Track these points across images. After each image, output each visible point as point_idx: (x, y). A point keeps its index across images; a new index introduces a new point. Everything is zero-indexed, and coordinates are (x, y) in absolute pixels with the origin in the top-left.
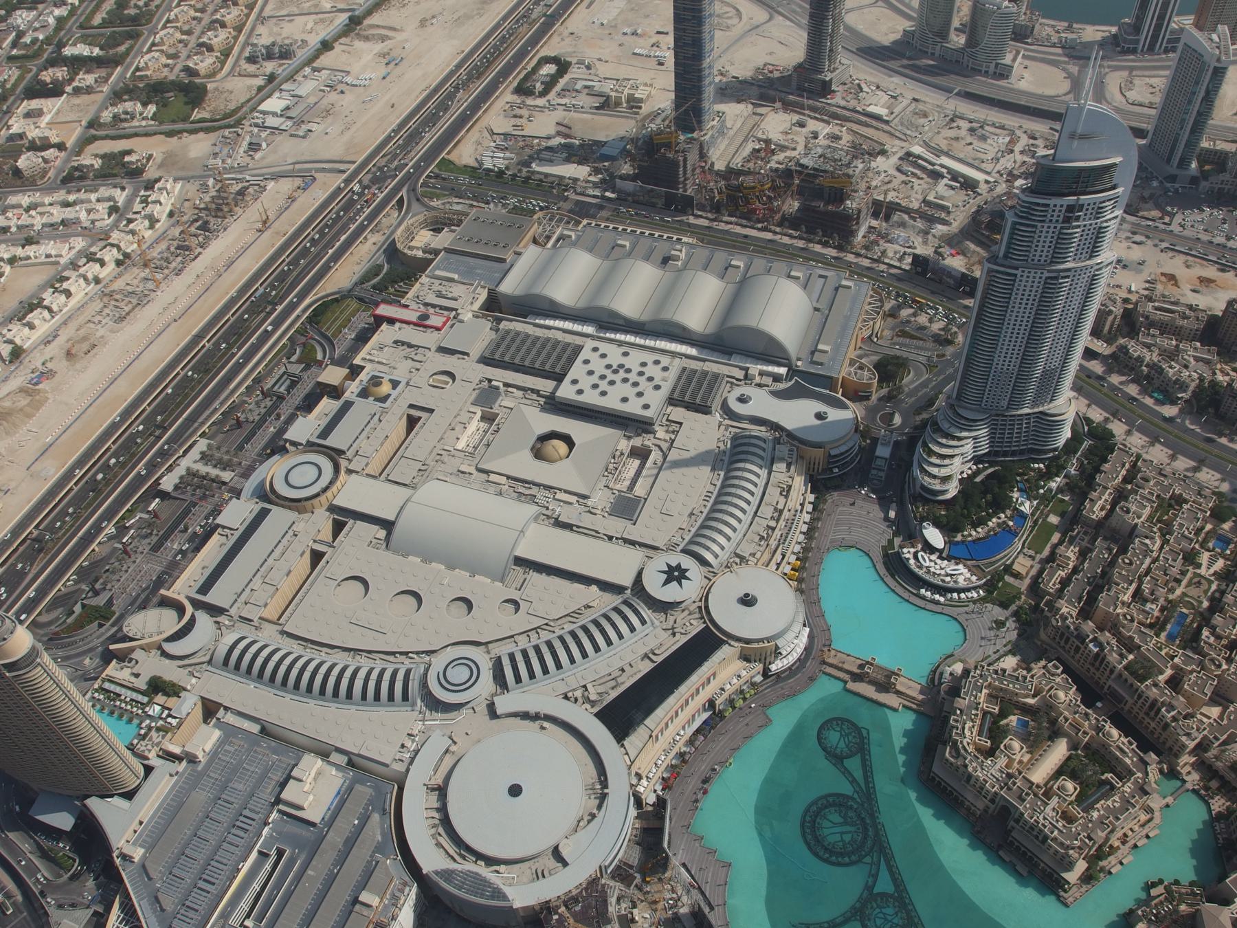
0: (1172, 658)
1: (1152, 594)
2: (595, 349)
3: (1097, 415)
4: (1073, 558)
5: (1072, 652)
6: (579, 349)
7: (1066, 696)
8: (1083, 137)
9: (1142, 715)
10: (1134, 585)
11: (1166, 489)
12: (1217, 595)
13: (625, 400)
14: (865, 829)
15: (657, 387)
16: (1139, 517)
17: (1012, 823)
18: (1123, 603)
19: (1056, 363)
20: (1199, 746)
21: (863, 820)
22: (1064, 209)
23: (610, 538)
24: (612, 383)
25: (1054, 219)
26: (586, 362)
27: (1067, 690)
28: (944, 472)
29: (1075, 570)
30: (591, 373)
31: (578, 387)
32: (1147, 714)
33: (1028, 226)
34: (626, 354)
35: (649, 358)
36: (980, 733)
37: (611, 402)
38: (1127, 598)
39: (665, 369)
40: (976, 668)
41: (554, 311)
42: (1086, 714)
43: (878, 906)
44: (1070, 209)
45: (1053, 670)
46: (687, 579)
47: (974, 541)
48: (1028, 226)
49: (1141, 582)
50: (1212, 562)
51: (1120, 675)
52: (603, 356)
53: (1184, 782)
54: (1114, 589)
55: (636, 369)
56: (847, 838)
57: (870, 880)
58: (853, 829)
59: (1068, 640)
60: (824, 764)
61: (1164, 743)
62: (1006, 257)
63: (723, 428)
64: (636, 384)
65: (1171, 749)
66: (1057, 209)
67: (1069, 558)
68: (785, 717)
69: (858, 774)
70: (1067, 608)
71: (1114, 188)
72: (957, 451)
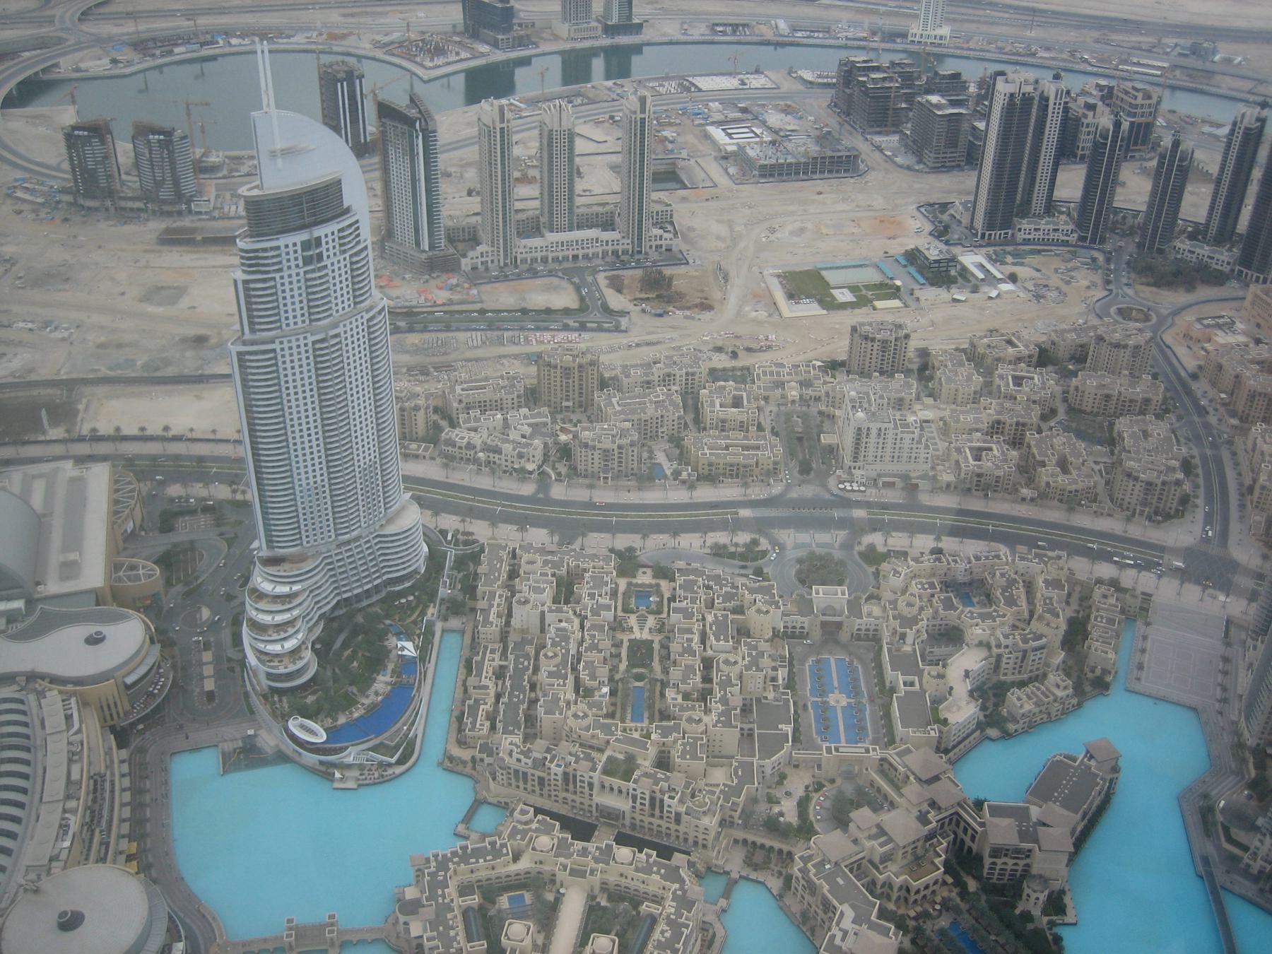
0: (648, 736)
1: (593, 677)
3: (449, 522)
4: (491, 684)
5: (537, 789)
8: (287, 152)
9: (647, 819)
10: (571, 678)
11: (557, 565)
12: (664, 652)
20: (722, 823)
22: (299, 248)
25: (293, 264)
27: (548, 831)
28: (290, 644)
29: (498, 697)
32: (653, 815)
33: (264, 281)
36: (470, 939)
38: (571, 696)
40: (428, 860)
42: (585, 849)
44: (306, 245)
48: (264, 281)
49: (574, 669)
50: (642, 621)
53: (728, 873)
61: (686, 840)
62: (253, 331)
65: (696, 843)
66: (291, 249)
67: (486, 687)
71: (348, 210)
72: (296, 613)
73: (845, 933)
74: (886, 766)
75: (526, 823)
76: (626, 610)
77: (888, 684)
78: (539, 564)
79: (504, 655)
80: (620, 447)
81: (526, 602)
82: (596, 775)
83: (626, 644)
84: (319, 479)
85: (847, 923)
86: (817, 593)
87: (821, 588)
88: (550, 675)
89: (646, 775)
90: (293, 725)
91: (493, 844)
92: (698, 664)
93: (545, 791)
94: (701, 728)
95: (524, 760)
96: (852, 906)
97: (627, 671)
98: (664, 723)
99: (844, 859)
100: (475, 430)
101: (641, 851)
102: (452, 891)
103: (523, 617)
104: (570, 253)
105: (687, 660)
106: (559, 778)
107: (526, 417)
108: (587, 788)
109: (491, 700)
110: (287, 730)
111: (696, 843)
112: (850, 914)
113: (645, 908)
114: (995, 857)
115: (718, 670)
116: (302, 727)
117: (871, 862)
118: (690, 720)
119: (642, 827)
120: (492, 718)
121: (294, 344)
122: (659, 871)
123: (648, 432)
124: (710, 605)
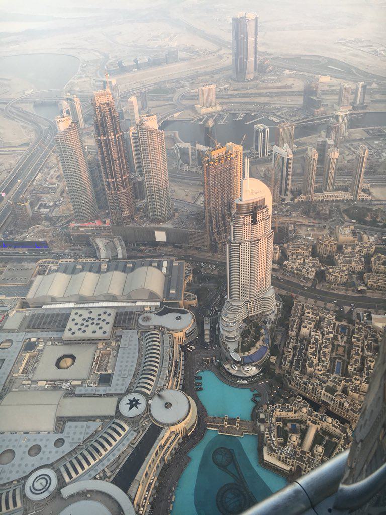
0: (341, 381)
2: (77, 314)
3: (284, 292)
4: (291, 351)
5: (303, 390)
6: (68, 315)
9: (337, 408)
13: (94, 332)
15: (108, 323)
17: (303, 472)
19: (264, 276)
23: (100, 395)
24: (87, 326)
26: (74, 320)
27: (306, 406)
29: (294, 356)
30: (76, 324)
31: (72, 332)
32: (339, 407)
34: (91, 312)
35: (101, 311)
37: (89, 334)
39: (109, 315)
41: (54, 300)
45: (299, 400)
46: (139, 404)
49: (319, 352)
51: (324, 394)
52: (81, 316)
55: (96, 318)
59: (300, 385)
63: (139, 334)
64: (98, 324)
67: (290, 352)
68: (197, 454)
71: (266, 207)
75: (299, 402)
76: (337, 333)
79: (297, 342)
80: (341, 275)
81: (306, 327)
82: (323, 392)
84: (247, 282)
88: (311, 354)
89: (339, 395)
92: (359, 358)
94: (359, 382)
95: (300, 380)
100: (294, 262)
101: (335, 420)
102: (274, 420)
103: (304, 331)
104: (331, 199)
105: (356, 357)
107: (311, 260)
109: (291, 356)
111: (353, 420)
113: (334, 439)
115: (367, 363)
118: (356, 379)
120: (291, 362)
121: (245, 245)
123: (351, 272)
124: (366, 337)
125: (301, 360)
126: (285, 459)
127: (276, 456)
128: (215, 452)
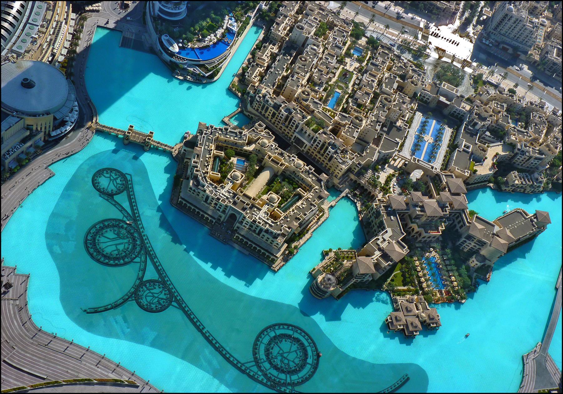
5: (270, 117)
7: (269, 142)
9: (315, 153)
10: (308, 75)
14: (134, 240)
16: (309, 34)
18: (302, 85)
21: (132, 234)
29: (269, 67)
32: (319, 152)
38: (304, 82)
43: (148, 289)
47: (200, 49)
51: (302, 130)
54: (296, 76)
56: (121, 247)
57: (141, 273)
58: (126, 241)
59: (267, 108)
60: (99, 200)
65: (332, 173)
69: (126, 205)
70: (266, 90)
73: (384, 240)
74: (437, 177)
77: (456, 143)
78: (316, 12)
83: (340, 70)
85: (387, 237)
86: (444, 86)
87: (447, 85)
90: (164, 38)
91: (241, 133)
93: (273, 120)
96: (393, 231)
97: (336, 82)
98: (344, 114)
99: (398, 210)
106: (283, 117)
108: (294, 127)
110: (160, 39)
112: (390, 233)
114: (468, 239)
116: (168, 41)
117: (410, 216)
119: (311, 155)
122: (312, 177)
125: (279, 74)
126: (214, 202)
127: (201, 195)
128: (100, 173)
